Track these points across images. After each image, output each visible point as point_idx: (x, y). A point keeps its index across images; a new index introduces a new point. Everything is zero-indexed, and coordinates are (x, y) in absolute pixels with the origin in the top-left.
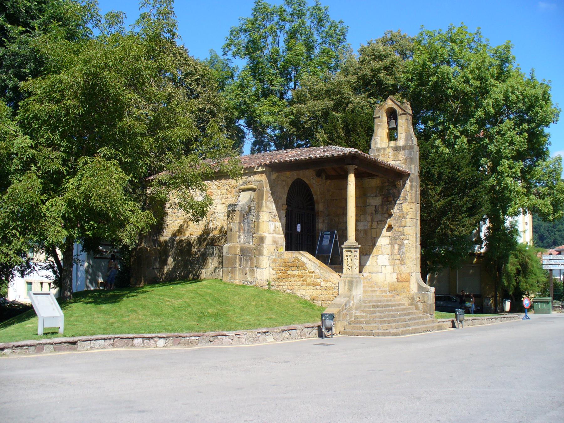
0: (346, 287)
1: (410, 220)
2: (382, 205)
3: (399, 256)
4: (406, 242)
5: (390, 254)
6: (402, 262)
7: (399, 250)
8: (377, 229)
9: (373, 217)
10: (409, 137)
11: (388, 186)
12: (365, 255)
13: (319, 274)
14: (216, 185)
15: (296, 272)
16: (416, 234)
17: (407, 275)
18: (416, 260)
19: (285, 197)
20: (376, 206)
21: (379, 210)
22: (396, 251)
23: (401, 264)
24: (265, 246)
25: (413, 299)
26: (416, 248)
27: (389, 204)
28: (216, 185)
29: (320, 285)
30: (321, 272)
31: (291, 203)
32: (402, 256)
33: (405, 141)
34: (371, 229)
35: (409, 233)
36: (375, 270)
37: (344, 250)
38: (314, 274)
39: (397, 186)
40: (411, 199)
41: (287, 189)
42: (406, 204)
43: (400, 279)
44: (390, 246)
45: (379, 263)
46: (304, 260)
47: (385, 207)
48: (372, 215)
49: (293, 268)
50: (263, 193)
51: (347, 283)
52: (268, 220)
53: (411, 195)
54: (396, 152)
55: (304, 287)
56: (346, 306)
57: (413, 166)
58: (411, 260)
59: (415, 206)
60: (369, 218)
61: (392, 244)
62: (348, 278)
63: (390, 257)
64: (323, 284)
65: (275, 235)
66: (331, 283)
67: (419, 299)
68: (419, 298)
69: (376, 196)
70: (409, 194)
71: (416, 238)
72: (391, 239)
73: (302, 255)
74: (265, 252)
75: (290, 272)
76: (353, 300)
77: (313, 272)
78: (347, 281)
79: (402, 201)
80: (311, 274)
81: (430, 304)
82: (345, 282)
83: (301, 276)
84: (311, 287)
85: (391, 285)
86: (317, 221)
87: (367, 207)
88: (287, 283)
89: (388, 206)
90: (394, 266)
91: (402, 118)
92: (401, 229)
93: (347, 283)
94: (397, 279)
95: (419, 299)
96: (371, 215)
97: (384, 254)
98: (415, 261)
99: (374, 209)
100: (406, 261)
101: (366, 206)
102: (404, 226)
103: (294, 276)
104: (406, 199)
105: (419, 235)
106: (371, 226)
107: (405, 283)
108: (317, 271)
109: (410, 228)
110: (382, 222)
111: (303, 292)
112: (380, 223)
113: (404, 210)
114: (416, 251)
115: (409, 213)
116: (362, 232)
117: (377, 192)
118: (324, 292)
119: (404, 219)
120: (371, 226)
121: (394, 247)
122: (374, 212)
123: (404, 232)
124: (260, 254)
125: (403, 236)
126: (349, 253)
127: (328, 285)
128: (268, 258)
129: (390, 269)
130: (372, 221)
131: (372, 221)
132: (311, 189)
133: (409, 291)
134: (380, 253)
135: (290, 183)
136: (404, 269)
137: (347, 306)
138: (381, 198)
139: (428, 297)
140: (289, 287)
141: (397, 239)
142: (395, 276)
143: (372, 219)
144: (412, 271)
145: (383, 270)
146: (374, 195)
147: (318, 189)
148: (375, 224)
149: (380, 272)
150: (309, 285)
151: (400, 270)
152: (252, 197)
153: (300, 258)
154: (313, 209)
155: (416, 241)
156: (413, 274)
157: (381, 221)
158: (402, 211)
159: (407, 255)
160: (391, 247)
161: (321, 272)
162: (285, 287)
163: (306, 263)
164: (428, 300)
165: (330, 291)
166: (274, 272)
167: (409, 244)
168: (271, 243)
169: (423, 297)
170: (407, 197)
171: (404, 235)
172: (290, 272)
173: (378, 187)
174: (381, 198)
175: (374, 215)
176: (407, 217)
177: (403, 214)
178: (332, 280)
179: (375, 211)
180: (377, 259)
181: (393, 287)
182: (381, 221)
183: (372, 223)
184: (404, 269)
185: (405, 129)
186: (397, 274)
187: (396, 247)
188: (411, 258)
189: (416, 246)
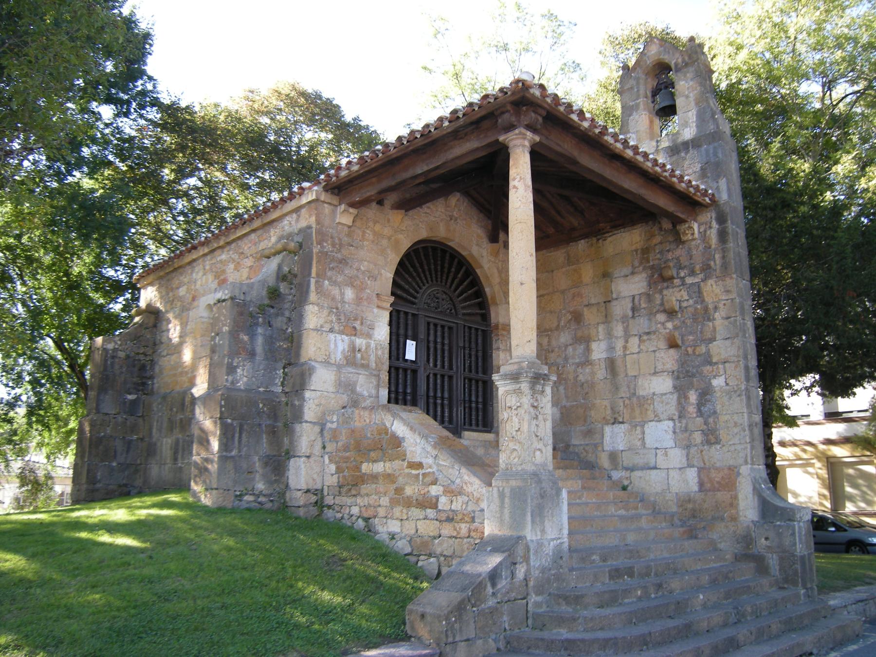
0: (507, 511)
1: (726, 322)
2: (649, 297)
3: (700, 420)
4: (718, 382)
5: (676, 417)
6: (711, 437)
7: (700, 405)
8: (641, 355)
9: (628, 326)
10: (708, 115)
11: (661, 243)
12: (613, 424)
13: (435, 469)
14: (234, 261)
15: (379, 467)
16: (746, 357)
17: (726, 471)
18: (751, 431)
19: (388, 275)
20: (634, 297)
21: (643, 305)
22: (692, 409)
23: (709, 443)
24: (307, 394)
25: (747, 540)
26: (749, 398)
27: (667, 287)
28: (234, 261)
29: (434, 506)
30: (438, 465)
31: (415, 298)
32: (711, 420)
33: (697, 126)
34: (625, 355)
35: (724, 355)
36: (639, 460)
37: (501, 391)
38: (421, 472)
39: (684, 238)
40: (725, 266)
41: (394, 259)
42: (710, 282)
43: (708, 486)
44: (675, 396)
45: (650, 442)
46: (399, 428)
47: (657, 296)
48: (624, 319)
49: (372, 454)
50: (312, 259)
51: (507, 500)
52: (327, 327)
53: (724, 257)
54: (674, 158)
55: (397, 511)
56: (494, 585)
57: (723, 183)
58: (736, 430)
59: (737, 285)
60: (619, 330)
61: (680, 390)
62: (513, 483)
63: (678, 425)
64: (443, 502)
65: (350, 369)
66: (466, 499)
67: (768, 543)
68: (767, 539)
69: (633, 273)
70: (717, 256)
71: (747, 368)
72: (678, 378)
73: (395, 416)
74: (310, 412)
75: (365, 468)
76: (526, 559)
77: (420, 465)
78: (507, 491)
79: (701, 276)
80: (414, 472)
81: (802, 558)
82: (502, 495)
83: (390, 478)
84: (416, 512)
85: (684, 501)
86: (494, 346)
87: (614, 303)
88: (359, 500)
89: (665, 292)
90: (688, 447)
91: (685, 76)
92: (703, 349)
93: (507, 500)
94: (701, 484)
95: (768, 543)
96: (623, 323)
97: (662, 417)
98: (747, 432)
99: (630, 305)
100: (723, 434)
101: (609, 301)
102: (713, 339)
103: (374, 477)
104: (709, 267)
105: (753, 363)
106: (625, 348)
107: (722, 496)
108: (430, 461)
109: (728, 342)
110: (653, 337)
111: (394, 526)
112: (645, 337)
113: (709, 300)
114: (749, 406)
115: (721, 305)
116: (603, 366)
117: (636, 263)
118: (447, 530)
119: (709, 320)
120: (625, 348)
121: (686, 398)
122: (630, 314)
123: (710, 356)
124: (298, 416)
125: (709, 368)
126: (512, 401)
127: (457, 505)
128: (317, 429)
129: (677, 457)
130: (627, 336)
131: (627, 336)
132: (478, 271)
133: (734, 519)
134: (651, 415)
135: (406, 244)
136: (717, 456)
137: (502, 584)
138: (644, 275)
139: (793, 534)
140: (363, 509)
141: (693, 376)
142: (692, 475)
143: (626, 330)
144: (741, 461)
145: (661, 462)
146: (630, 269)
147: (495, 271)
148: (634, 342)
149: (652, 465)
150: (408, 503)
151: (706, 458)
152: (286, 269)
153: (388, 425)
154: (485, 317)
155: (748, 379)
156: (745, 470)
157: (648, 333)
158: (703, 301)
159: (723, 418)
160: (679, 399)
161: (438, 465)
162: (355, 510)
163: (403, 438)
164: (795, 544)
165: (463, 526)
166: (333, 468)
167: (728, 387)
168: (332, 389)
169: (780, 535)
170: (712, 263)
171: (711, 363)
172: (365, 468)
173: (636, 251)
174: (644, 275)
175: (631, 321)
176: (717, 315)
177: (706, 309)
178: (469, 489)
179: (634, 309)
180: (643, 433)
181: (690, 506)
182: (648, 333)
183: (627, 342)
184: (717, 456)
185: (695, 100)
186: (700, 470)
187: (693, 397)
188: (736, 424)
189: (747, 389)
